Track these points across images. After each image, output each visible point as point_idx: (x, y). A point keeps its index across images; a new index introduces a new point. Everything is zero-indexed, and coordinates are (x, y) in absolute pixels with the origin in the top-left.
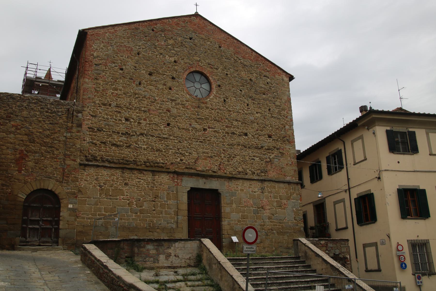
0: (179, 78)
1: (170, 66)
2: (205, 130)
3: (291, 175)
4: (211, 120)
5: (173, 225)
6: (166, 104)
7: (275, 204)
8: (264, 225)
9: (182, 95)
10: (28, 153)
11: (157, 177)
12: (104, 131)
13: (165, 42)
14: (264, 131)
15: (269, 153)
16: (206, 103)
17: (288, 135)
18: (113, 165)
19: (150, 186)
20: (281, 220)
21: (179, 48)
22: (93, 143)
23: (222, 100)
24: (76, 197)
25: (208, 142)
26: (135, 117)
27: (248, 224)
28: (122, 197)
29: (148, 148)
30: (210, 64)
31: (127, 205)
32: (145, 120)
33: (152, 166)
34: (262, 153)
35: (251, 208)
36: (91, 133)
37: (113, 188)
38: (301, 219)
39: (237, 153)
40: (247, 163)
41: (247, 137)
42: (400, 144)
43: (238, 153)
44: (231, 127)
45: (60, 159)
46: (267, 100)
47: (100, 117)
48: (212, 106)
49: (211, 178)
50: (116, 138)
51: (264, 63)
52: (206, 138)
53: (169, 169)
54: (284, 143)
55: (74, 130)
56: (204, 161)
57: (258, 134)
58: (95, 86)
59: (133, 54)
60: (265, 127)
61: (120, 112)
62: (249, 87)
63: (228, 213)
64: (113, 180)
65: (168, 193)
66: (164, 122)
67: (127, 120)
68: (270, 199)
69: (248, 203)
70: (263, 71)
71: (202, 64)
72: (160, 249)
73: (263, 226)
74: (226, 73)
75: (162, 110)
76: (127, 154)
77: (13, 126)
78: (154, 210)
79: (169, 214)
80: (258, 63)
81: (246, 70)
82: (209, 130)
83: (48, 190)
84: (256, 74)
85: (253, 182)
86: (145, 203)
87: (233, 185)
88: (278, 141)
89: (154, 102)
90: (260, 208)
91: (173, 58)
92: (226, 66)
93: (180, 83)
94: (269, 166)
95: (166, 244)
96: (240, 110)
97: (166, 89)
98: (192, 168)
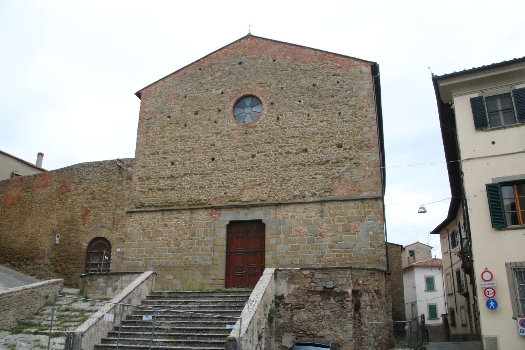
0: (225, 108)
1: (216, 99)
2: (253, 156)
3: (369, 189)
4: (261, 144)
5: (209, 262)
6: (211, 139)
7: (340, 229)
8: (322, 256)
9: (227, 125)
10: (90, 208)
11: (195, 214)
12: (152, 179)
13: (212, 76)
14: (330, 142)
15: (339, 166)
16: (255, 127)
17: (367, 138)
18: (153, 209)
19: (187, 224)
20: (348, 248)
21: (226, 77)
22: (142, 192)
23: (275, 118)
24: (124, 242)
25: (257, 169)
26: (179, 159)
27: (300, 256)
28: (161, 238)
29: (190, 187)
30: (261, 83)
31: (166, 246)
32: (189, 160)
33: (194, 205)
34: (327, 169)
35: (305, 237)
36: (140, 183)
37: (154, 230)
38: (382, 245)
39: (293, 175)
40: (306, 184)
41: (306, 154)
42: (501, 113)
43: (294, 174)
44: (286, 146)
45: (112, 210)
46: (337, 102)
47: (149, 166)
48: (262, 128)
49: (253, 208)
50: (162, 184)
51: (332, 60)
52: (255, 164)
53: (211, 204)
54: (361, 149)
55: (124, 183)
56: (250, 190)
57: (322, 147)
58: (145, 139)
59: (180, 99)
60: (332, 136)
61: (166, 158)
62: (311, 94)
63: (272, 245)
64: (154, 223)
65: (205, 230)
66: (208, 158)
67: (173, 164)
68: (333, 224)
69: (301, 231)
70: (331, 70)
71: (253, 86)
72: (109, 282)
73: (320, 257)
74: (281, 86)
75: (207, 146)
76: (173, 196)
77: (82, 188)
78: (191, 248)
79: (205, 251)
80: (325, 62)
81: (308, 76)
82: (258, 155)
83: (102, 238)
84: (322, 76)
85: (308, 206)
86: (182, 242)
87: (282, 212)
88: (351, 150)
89: (199, 140)
90: (318, 235)
91: (220, 90)
92: (281, 79)
93: (226, 113)
94: (336, 182)
95: (114, 277)
96: (298, 124)
97: (211, 123)
98: (235, 201)
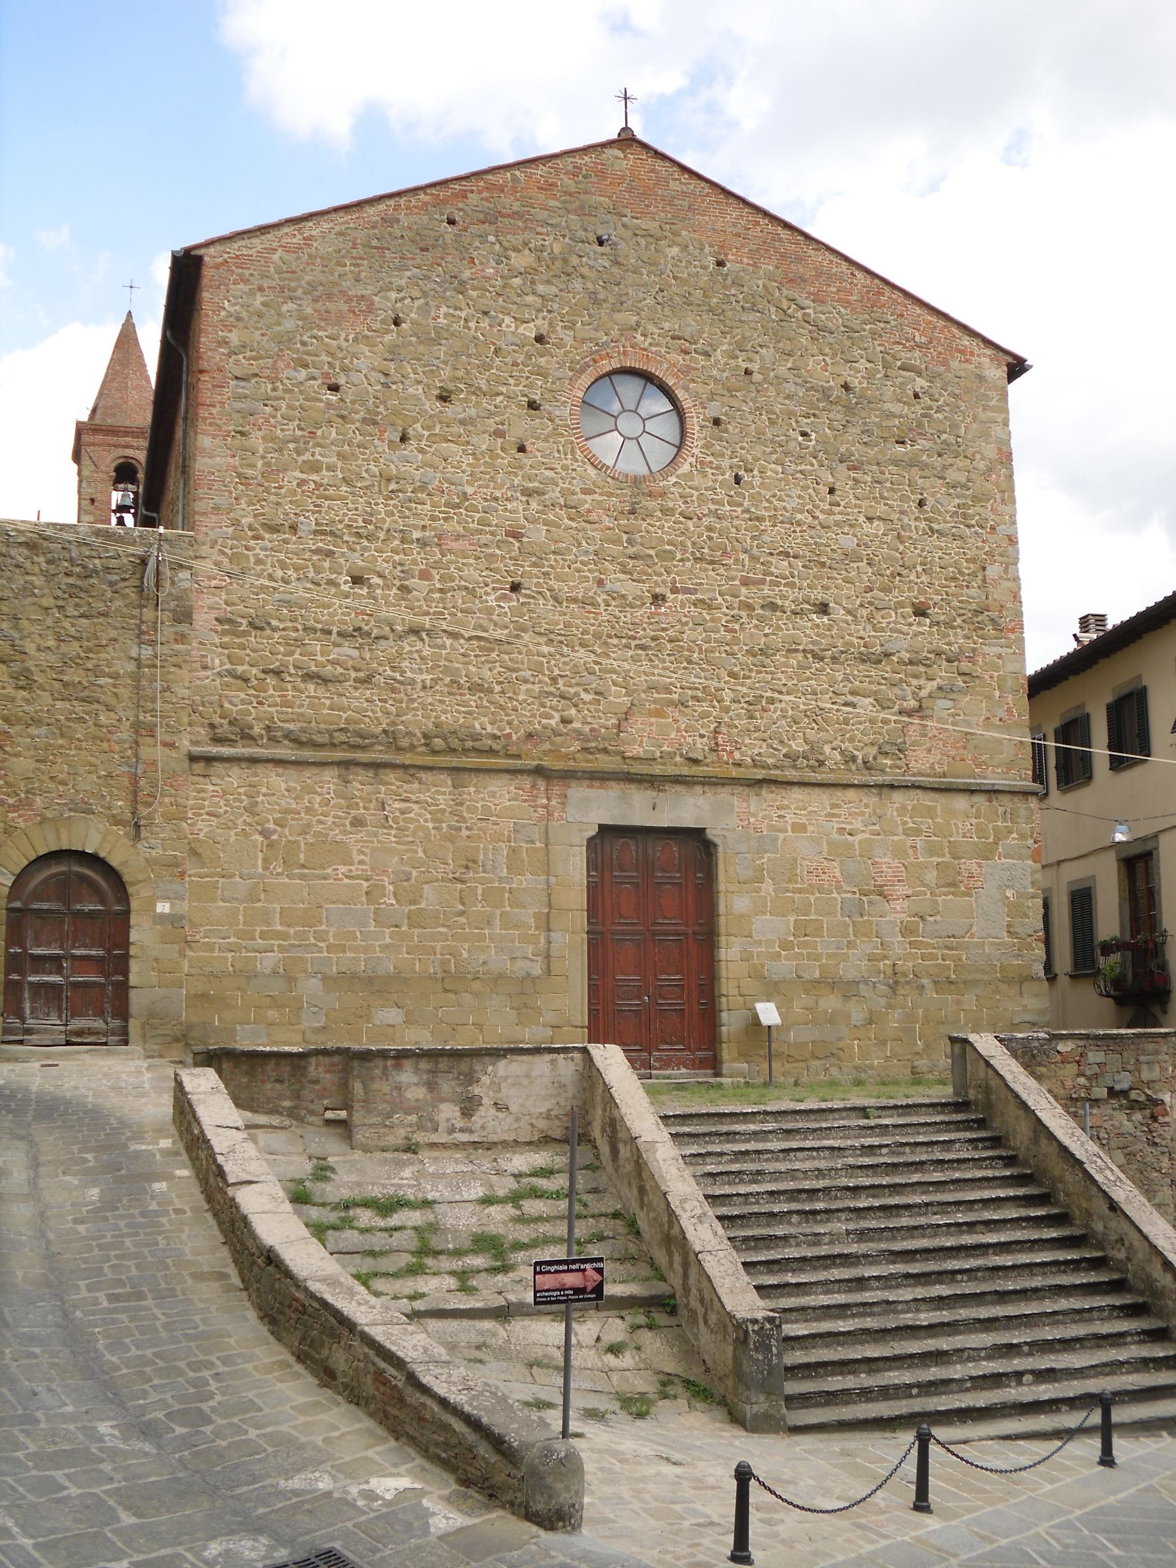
1: (521, 358)
2: (658, 599)
4: (682, 560)
7: (931, 876)
11: (472, 789)
12: (274, 629)
14: (896, 592)
15: (916, 676)
16: (663, 494)
18: (308, 754)
20: (953, 936)
22: (236, 677)
23: (727, 476)
24: (182, 874)
25: (669, 646)
26: (386, 568)
28: (343, 869)
29: (435, 681)
30: (680, 339)
31: (364, 899)
32: (425, 575)
34: (885, 679)
35: (835, 895)
36: (226, 639)
39: (785, 685)
41: (825, 619)
43: (789, 684)
44: (763, 582)
50: (319, 654)
54: (981, 632)
55: (167, 631)
56: (653, 720)
61: (330, 554)
62: (839, 416)
64: (309, 810)
66: (498, 581)
67: (357, 580)
71: (649, 340)
74: (744, 365)
75: (493, 534)
78: (462, 914)
79: (516, 926)
81: (827, 350)
86: (426, 887)
88: (953, 628)
89: (458, 506)
91: (531, 325)
92: (744, 337)
93: (557, 421)
96: (801, 512)
97: (503, 450)
